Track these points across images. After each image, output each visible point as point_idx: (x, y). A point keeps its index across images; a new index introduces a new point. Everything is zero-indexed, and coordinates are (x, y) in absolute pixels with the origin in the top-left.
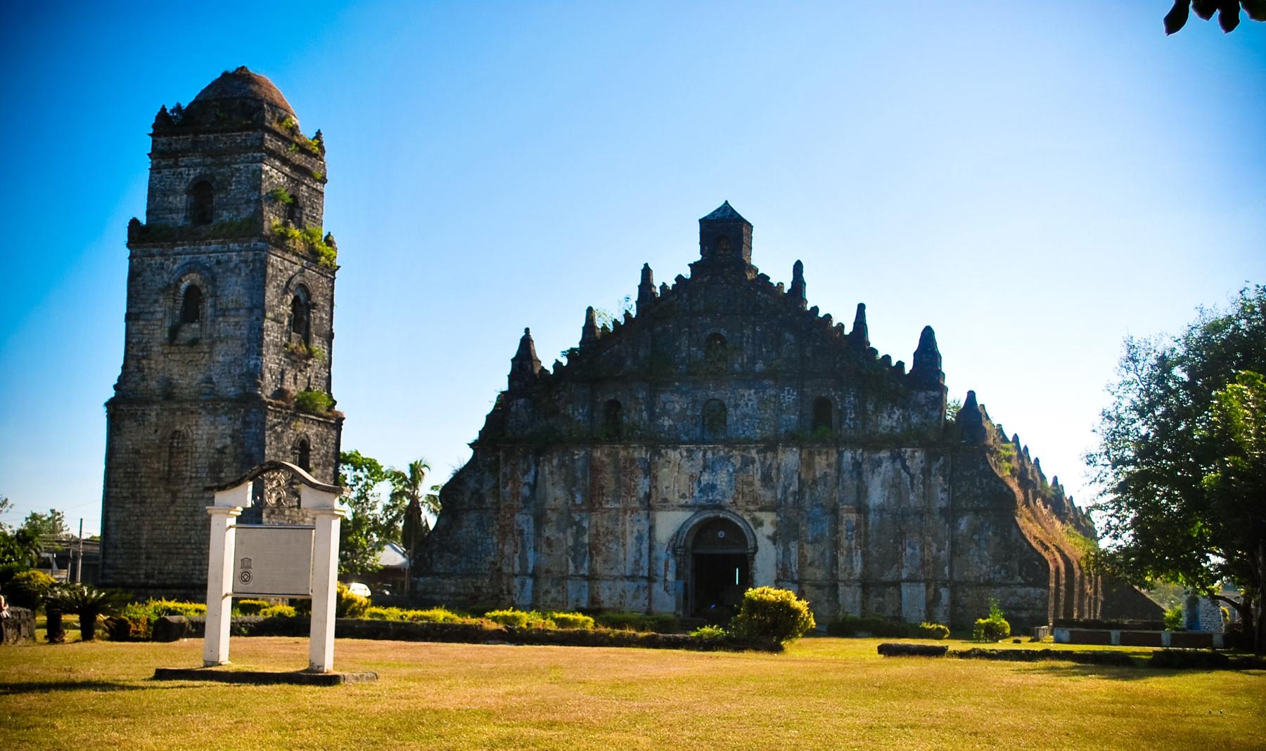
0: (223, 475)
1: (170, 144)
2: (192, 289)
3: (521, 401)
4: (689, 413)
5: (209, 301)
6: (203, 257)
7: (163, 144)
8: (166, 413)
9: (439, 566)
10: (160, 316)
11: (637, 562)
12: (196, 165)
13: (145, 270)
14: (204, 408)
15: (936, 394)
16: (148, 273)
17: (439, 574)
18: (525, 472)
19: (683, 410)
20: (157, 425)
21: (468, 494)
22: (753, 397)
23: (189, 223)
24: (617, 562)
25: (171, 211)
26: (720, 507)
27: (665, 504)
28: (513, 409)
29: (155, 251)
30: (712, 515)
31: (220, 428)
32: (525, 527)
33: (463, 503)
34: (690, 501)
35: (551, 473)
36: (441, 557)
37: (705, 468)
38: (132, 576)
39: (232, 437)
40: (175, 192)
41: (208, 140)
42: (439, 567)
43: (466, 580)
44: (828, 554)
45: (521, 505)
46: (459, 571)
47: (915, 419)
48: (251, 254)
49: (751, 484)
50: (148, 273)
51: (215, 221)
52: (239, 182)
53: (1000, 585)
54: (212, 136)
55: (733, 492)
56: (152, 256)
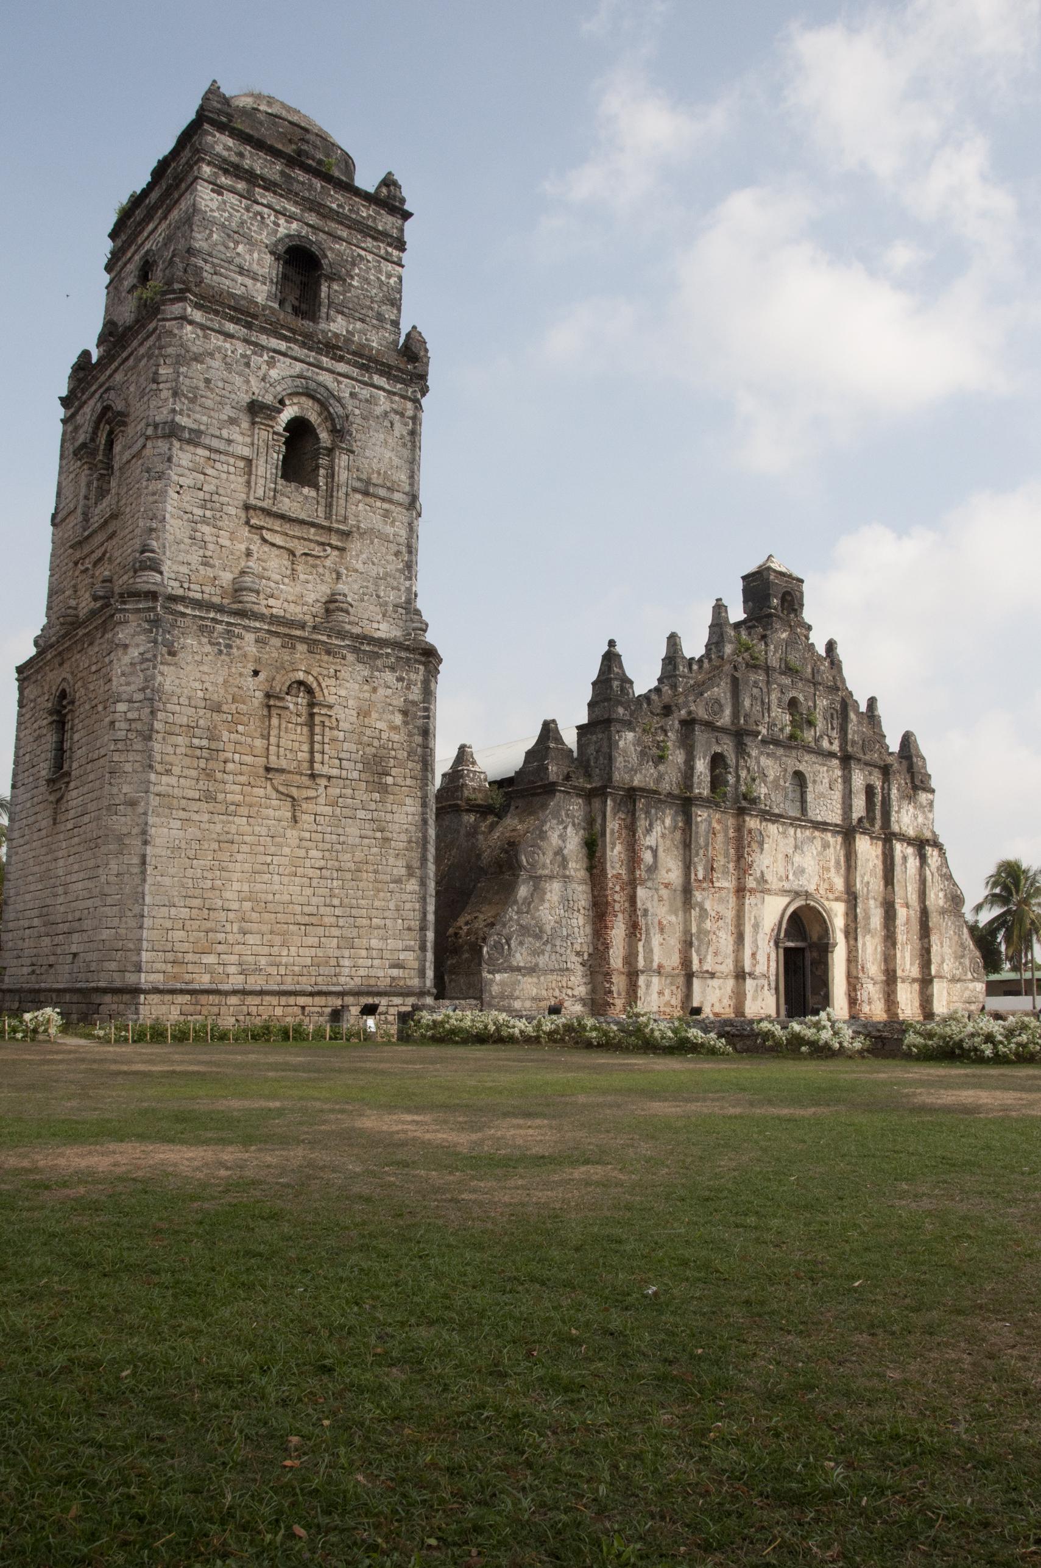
0: (390, 780)
1: (241, 155)
2: (299, 429)
3: (630, 735)
4: (782, 782)
5: (342, 460)
6: (326, 378)
7: (229, 149)
8: (276, 642)
9: (518, 955)
10: (246, 452)
11: (754, 955)
12: (291, 218)
13: (211, 355)
14: (355, 650)
15: (930, 796)
16: (216, 363)
17: (518, 969)
18: (649, 831)
19: (777, 779)
20: (258, 660)
21: (550, 855)
22: (825, 775)
23: (276, 306)
24: (726, 957)
25: (242, 271)
26: (807, 895)
27: (763, 889)
28: (621, 744)
29: (231, 327)
30: (803, 903)
31: (381, 691)
32: (649, 905)
33: (544, 866)
34: (787, 886)
35: (663, 836)
36: (521, 943)
37: (796, 847)
38: (208, 969)
39: (405, 713)
40: (251, 243)
41: (311, 187)
42: (520, 958)
43: (550, 977)
44: (879, 950)
45: (644, 875)
46: (541, 965)
47: (920, 820)
48: (409, 405)
49: (828, 870)
50: (216, 363)
51: (323, 325)
52: (367, 280)
53: (959, 980)
54: (318, 184)
55: (817, 877)
56: (229, 336)
